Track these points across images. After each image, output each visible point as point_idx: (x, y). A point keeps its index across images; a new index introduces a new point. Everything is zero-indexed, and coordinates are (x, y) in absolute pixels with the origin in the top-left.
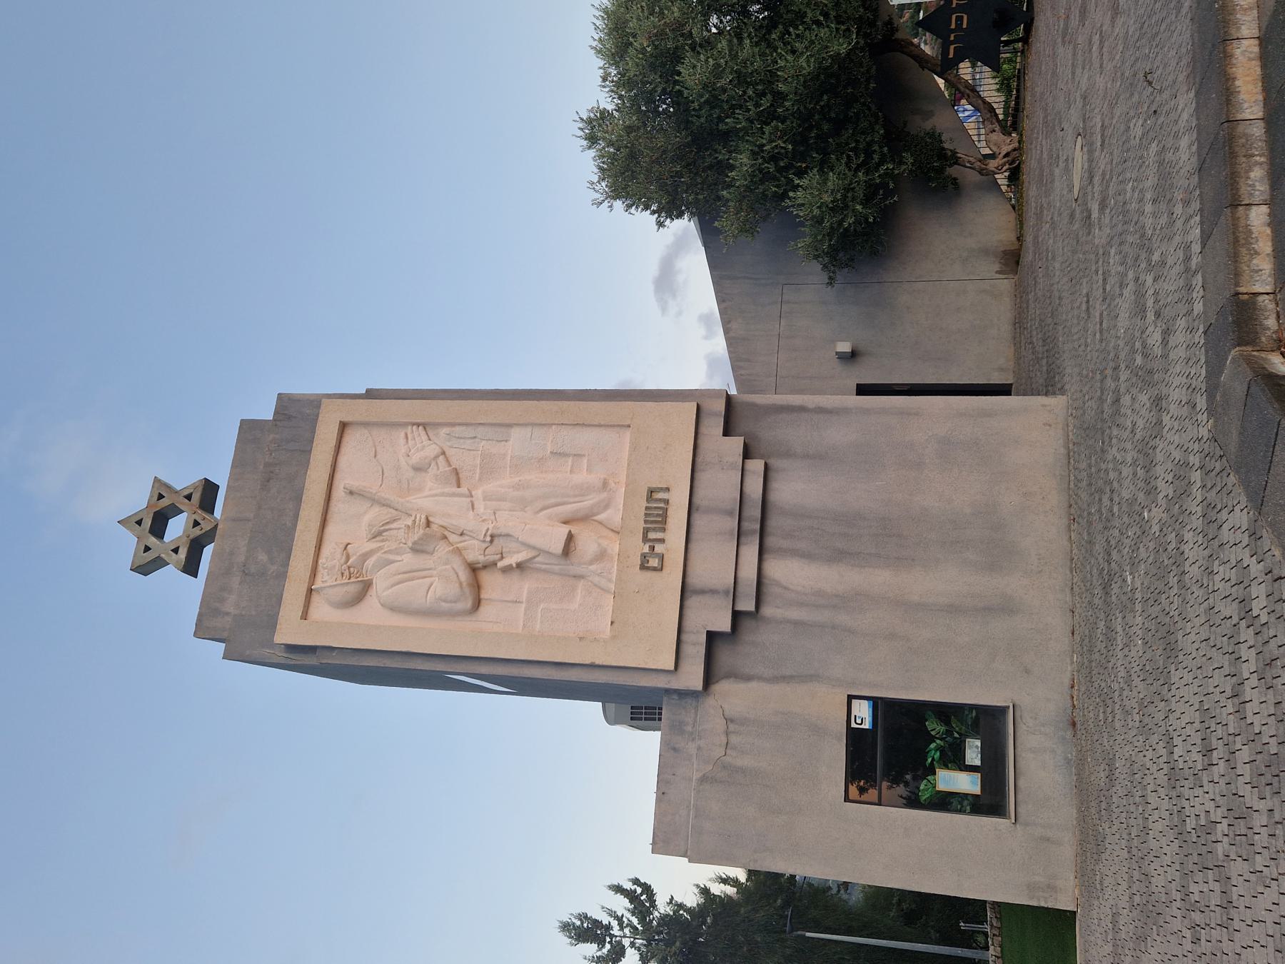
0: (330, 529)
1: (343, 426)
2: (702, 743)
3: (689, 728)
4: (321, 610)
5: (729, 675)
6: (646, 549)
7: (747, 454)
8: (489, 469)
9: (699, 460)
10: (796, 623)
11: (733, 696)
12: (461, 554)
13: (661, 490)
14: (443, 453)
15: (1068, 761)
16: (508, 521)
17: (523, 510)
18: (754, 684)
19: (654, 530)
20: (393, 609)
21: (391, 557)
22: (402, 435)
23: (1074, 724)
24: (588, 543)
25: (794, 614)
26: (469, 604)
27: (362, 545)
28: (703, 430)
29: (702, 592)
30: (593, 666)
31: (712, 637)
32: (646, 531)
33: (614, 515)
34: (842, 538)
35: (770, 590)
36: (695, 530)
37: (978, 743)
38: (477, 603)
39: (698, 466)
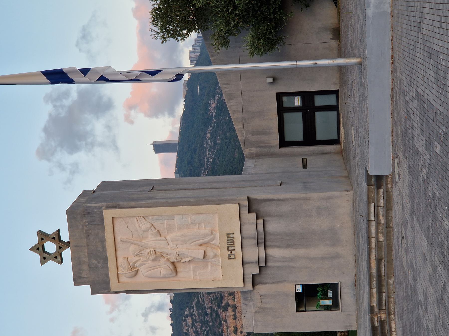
0: (118, 253)
1: (113, 218)
2: (254, 303)
3: (249, 299)
4: (123, 279)
5: (259, 284)
6: (229, 253)
7: (257, 218)
8: (170, 229)
9: (242, 222)
10: (278, 267)
11: (261, 289)
12: (169, 260)
13: (231, 234)
14: (153, 225)
15: (354, 295)
16: (182, 249)
17: (186, 244)
18: (267, 285)
19: (231, 247)
20: (149, 277)
21: (145, 263)
22: (136, 220)
23: (356, 286)
24: (210, 254)
25: (277, 264)
26: (175, 274)
27: (133, 259)
28: (242, 212)
29: (249, 263)
30: (218, 288)
31: (253, 275)
32: (228, 248)
33: (217, 242)
34: (289, 240)
35: (269, 258)
36: (244, 244)
37: (331, 292)
38: (177, 272)
39: (242, 224)
